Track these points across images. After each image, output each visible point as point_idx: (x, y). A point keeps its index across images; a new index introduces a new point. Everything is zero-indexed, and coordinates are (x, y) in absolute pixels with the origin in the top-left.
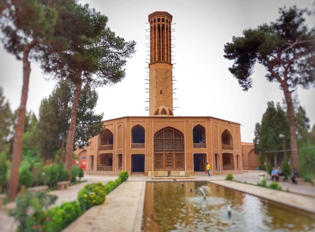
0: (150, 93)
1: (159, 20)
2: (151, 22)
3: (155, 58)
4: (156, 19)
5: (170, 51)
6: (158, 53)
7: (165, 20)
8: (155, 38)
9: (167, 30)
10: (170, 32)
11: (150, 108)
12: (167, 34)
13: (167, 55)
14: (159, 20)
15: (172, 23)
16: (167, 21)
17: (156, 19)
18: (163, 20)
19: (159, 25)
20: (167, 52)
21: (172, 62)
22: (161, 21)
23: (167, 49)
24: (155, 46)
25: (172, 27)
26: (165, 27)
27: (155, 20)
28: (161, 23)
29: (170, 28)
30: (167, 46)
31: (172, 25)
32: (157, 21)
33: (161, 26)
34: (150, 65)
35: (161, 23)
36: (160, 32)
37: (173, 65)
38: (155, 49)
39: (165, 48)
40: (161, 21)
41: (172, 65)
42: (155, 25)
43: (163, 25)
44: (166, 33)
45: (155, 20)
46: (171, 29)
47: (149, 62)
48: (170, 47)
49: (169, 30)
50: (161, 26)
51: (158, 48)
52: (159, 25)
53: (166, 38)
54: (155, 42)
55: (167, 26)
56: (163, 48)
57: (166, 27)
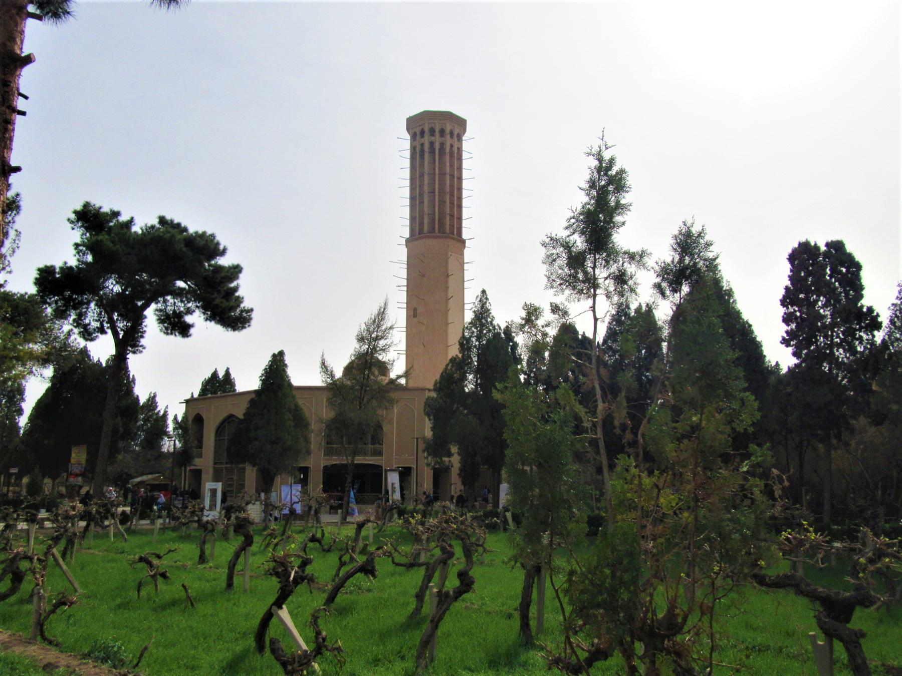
0: (407, 311)
1: (432, 132)
2: (414, 138)
3: (421, 224)
4: (426, 130)
5: (460, 207)
6: (429, 214)
7: (448, 131)
8: (422, 175)
9: (452, 156)
10: (460, 159)
11: (406, 351)
12: (452, 166)
13: (452, 216)
14: (432, 132)
15: (464, 138)
16: (452, 134)
17: (426, 130)
18: (442, 132)
19: (432, 144)
20: (452, 208)
21: (464, 236)
22: (437, 134)
23: (452, 203)
24: (421, 195)
25: (466, 146)
26: (445, 150)
27: (422, 133)
28: (437, 139)
29: (460, 150)
30: (450, 195)
31: (464, 143)
32: (426, 136)
33: (437, 147)
34: (407, 241)
35: (437, 139)
36: (434, 160)
37: (468, 243)
38: (421, 203)
39: (445, 202)
40: (437, 134)
41: (463, 242)
42: (422, 145)
43: (442, 145)
44: (448, 164)
45: (422, 133)
46: (462, 151)
47: (407, 236)
48: (460, 198)
49: (457, 157)
50: (437, 147)
51: (429, 201)
52: (432, 144)
53: (448, 177)
54: (421, 186)
55: (452, 146)
56: (442, 202)
57: (448, 148)
